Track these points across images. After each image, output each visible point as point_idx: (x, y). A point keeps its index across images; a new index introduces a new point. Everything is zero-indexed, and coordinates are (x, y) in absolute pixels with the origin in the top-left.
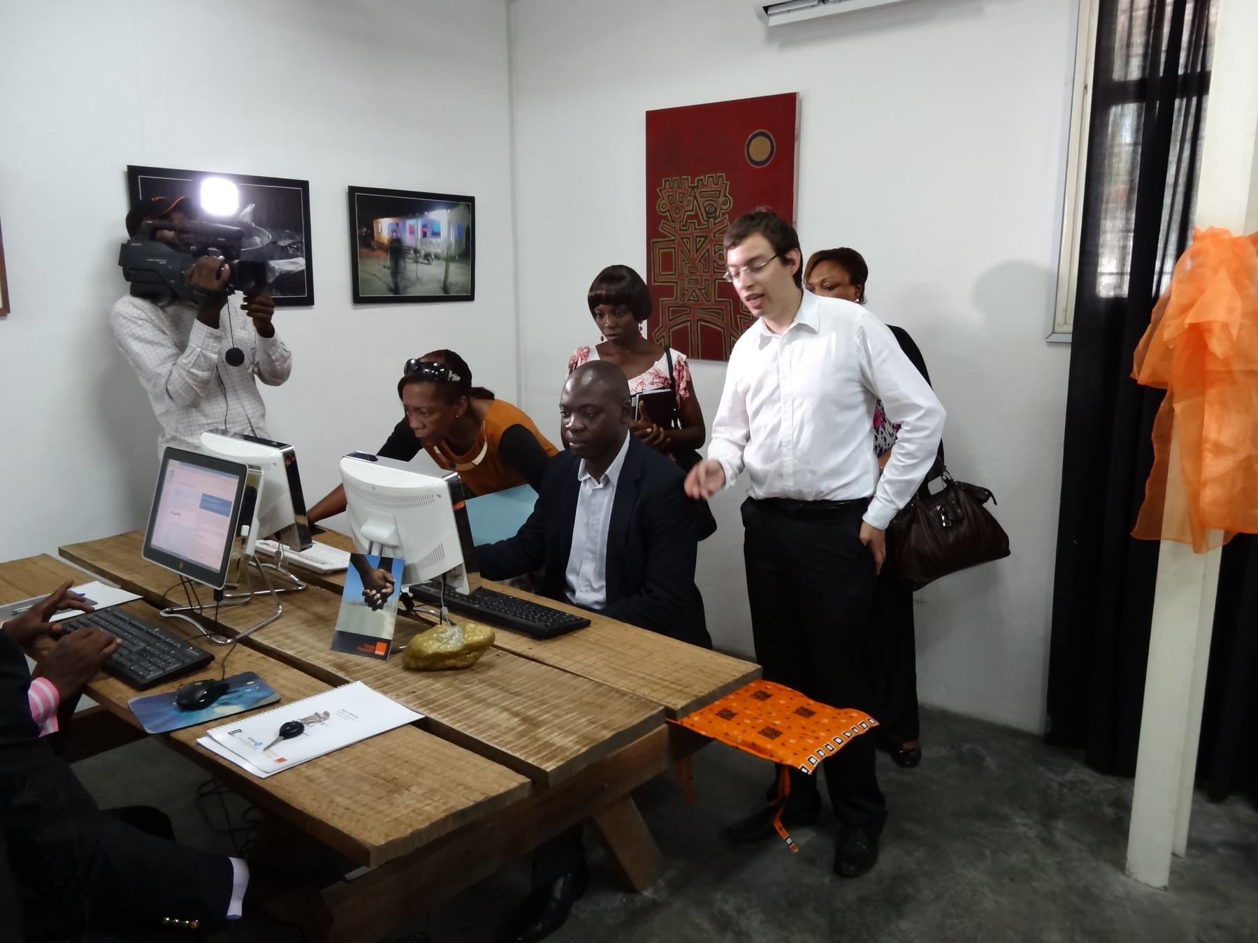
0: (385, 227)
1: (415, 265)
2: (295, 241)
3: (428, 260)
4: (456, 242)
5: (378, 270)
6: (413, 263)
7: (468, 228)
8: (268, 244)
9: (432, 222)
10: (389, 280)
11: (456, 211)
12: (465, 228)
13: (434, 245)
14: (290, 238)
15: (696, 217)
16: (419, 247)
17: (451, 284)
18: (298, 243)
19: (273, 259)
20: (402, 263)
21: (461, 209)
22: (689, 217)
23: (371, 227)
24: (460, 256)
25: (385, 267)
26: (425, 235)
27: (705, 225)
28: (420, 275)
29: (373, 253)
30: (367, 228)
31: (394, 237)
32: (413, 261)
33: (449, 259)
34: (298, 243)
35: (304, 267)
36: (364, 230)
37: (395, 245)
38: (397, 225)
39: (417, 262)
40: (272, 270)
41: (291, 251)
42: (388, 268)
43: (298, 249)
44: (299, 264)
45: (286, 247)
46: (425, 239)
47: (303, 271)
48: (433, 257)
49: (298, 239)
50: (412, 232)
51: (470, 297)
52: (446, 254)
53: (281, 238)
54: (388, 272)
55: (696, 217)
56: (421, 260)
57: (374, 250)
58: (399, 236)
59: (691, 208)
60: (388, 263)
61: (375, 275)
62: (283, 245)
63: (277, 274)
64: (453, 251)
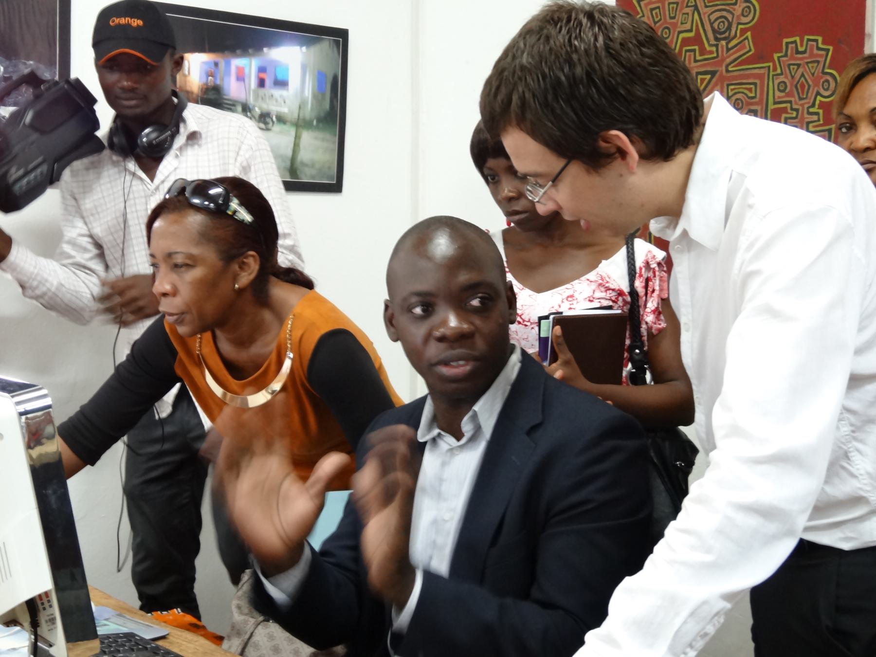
3: (266, 123)
4: (314, 96)
7: (335, 78)
9: (275, 64)
13: (277, 101)
16: (251, 101)
17: (303, 164)
24: (320, 120)
26: (261, 83)
31: (211, 84)
33: (301, 124)
38: (216, 64)
46: (261, 91)
48: (274, 119)
50: (241, 77)
51: (336, 187)
52: (296, 116)
58: (218, 82)
64: (309, 111)
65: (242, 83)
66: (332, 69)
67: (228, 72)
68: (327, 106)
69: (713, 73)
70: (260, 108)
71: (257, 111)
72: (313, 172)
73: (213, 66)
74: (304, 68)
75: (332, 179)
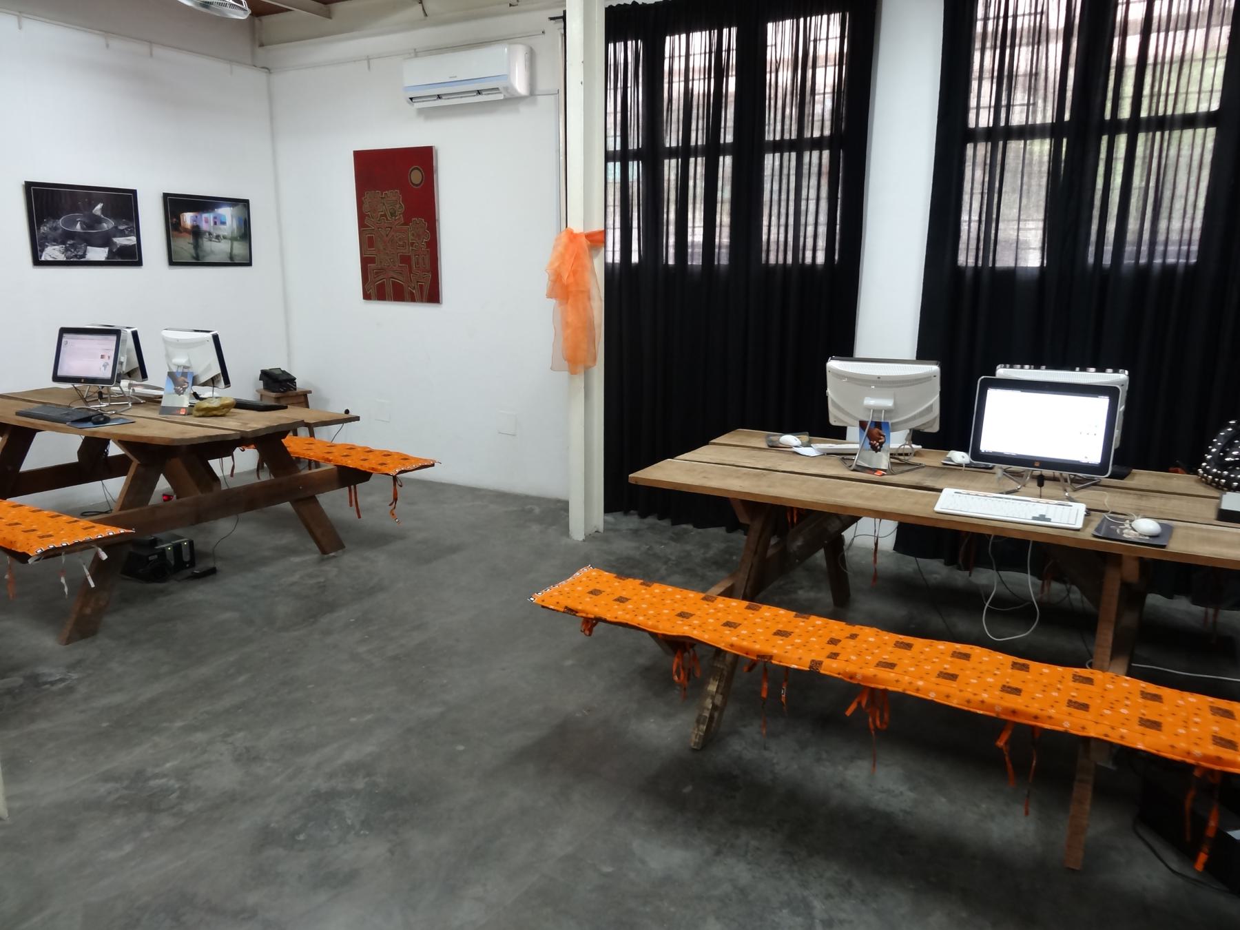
0: (188, 218)
4: (237, 228)
5: (185, 245)
7: (245, 219)
8: (112, 228)
9: (220, 215)
10: (192, 251)
11: (236, 208)
16: (212, 231)
17: (235, 255)
19: (115, 237)
20: (200, 240)
21: (240, 206)
23: (179, 219)
25: (189, 243)
26: (215, 223)
33: (233, 239)
35: (136, 243)
36: (175, 220)
38: (196, 217)
39: (211, 240)
40: (115, 244)
41: (127, 232)
44: (132, 240)
49: (131, 225)
50: (207, 221)
51: (249, 264)
52: (230, 235)
53: (120, 225)
56: (213, 239)
57: (181, 232)
60: (191, 241)
61: (182, 248)
64: (236, 233)
74: (232, 216)
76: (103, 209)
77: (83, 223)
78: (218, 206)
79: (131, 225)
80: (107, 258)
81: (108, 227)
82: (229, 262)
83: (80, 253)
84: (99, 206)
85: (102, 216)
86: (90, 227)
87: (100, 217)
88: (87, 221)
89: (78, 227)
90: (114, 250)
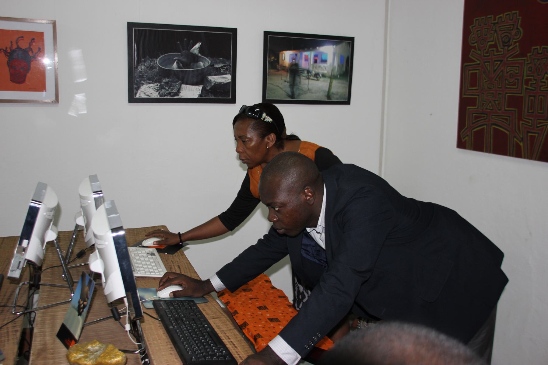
0: (287, 57)
1: (307, 81)
2: (226, 65)
3: (317, 78)
4: (339, 66)
6: (305, 79)
7: (348, 58)
8: (208, 66)
9: (322, 53)
10: (288, 90)
11: (339, 46)
12: (346, 57)
13: (322, 68)
14: (223, 63)
15: (495, 46)
16: (311, 69)
17: (333, 93)
18: (227, 66)
19: (210, 75)
20: (297, 79)
21: (344, 44)
22: (491, 46)
24: (341, 75)
25: (285, 81)
26: (315, 61)
27: (501, 52)
28: (310, 87)
29: (277, 73)
30: (275, 58)
31: (294, 63)
32: (306, 78)
33: (332, 77)
34: (227, 66)
36: (273, 58)
37: (294, 67)
38: (296, 55)
39: (308, 79)
40: (210, 82)
41: (222, 71)
42: (288, 82)
43: (227, 69)
44: (228, 78)
45: (219, 68)
46: (316, 65)
47: (230, 82)
48: (321, 76)
49: (228, 63)
50: (307, 59)
51: (348, 102)
52: (330, 74)
53: (216, 63)
54: (287, 84)
55: (495, 46)
56: (312, 77)
57: (278, 70)
58: (297, 62)
59: (492, 39)
60: (288, 79)
62: (218, 67)
63: (213, 84)
64: (336, 72)
65: (307, 62)
66: (346, 54)
67: (301, 58)
68: (344, 69)
69: (501, 61)
70: (315, 71)
71: (313, 73)
72: (337, 97)
73: (295, 56)
74: (334, 54)
75: (346, 99)
76: (201, 49)
77: (179, 62)
78: (320, 44)
79: (228, 63)
80: (201, 96)
81: (204, 66)
82: (326, 100)
83: (174, 91)
84: (198, 45)
85: (200, 55)
86: (186, 65)
87: (197, 56)
88: (184, 60)
89: (175, 65)
90: (208, 88)
